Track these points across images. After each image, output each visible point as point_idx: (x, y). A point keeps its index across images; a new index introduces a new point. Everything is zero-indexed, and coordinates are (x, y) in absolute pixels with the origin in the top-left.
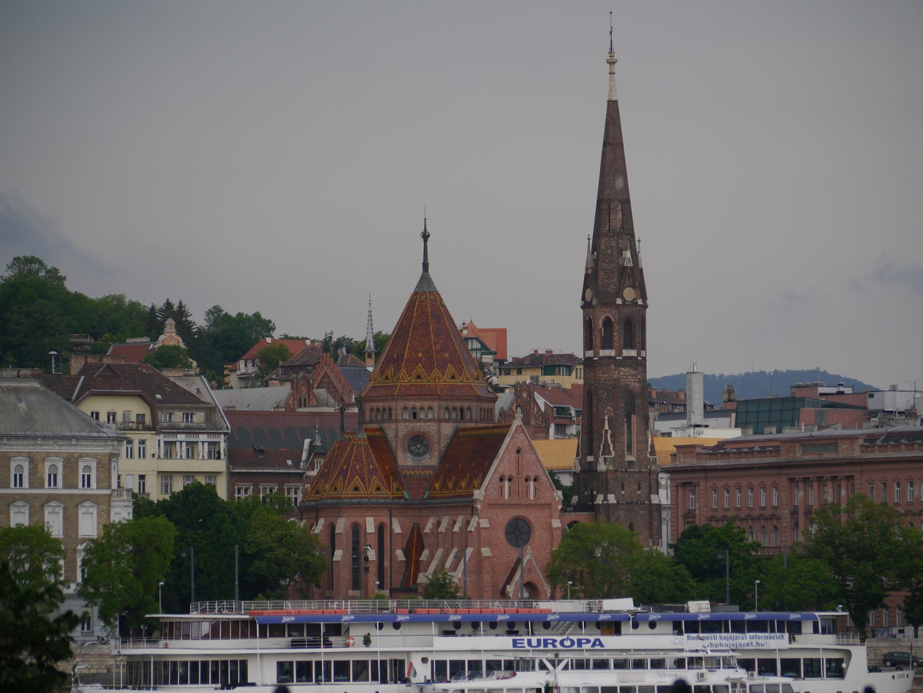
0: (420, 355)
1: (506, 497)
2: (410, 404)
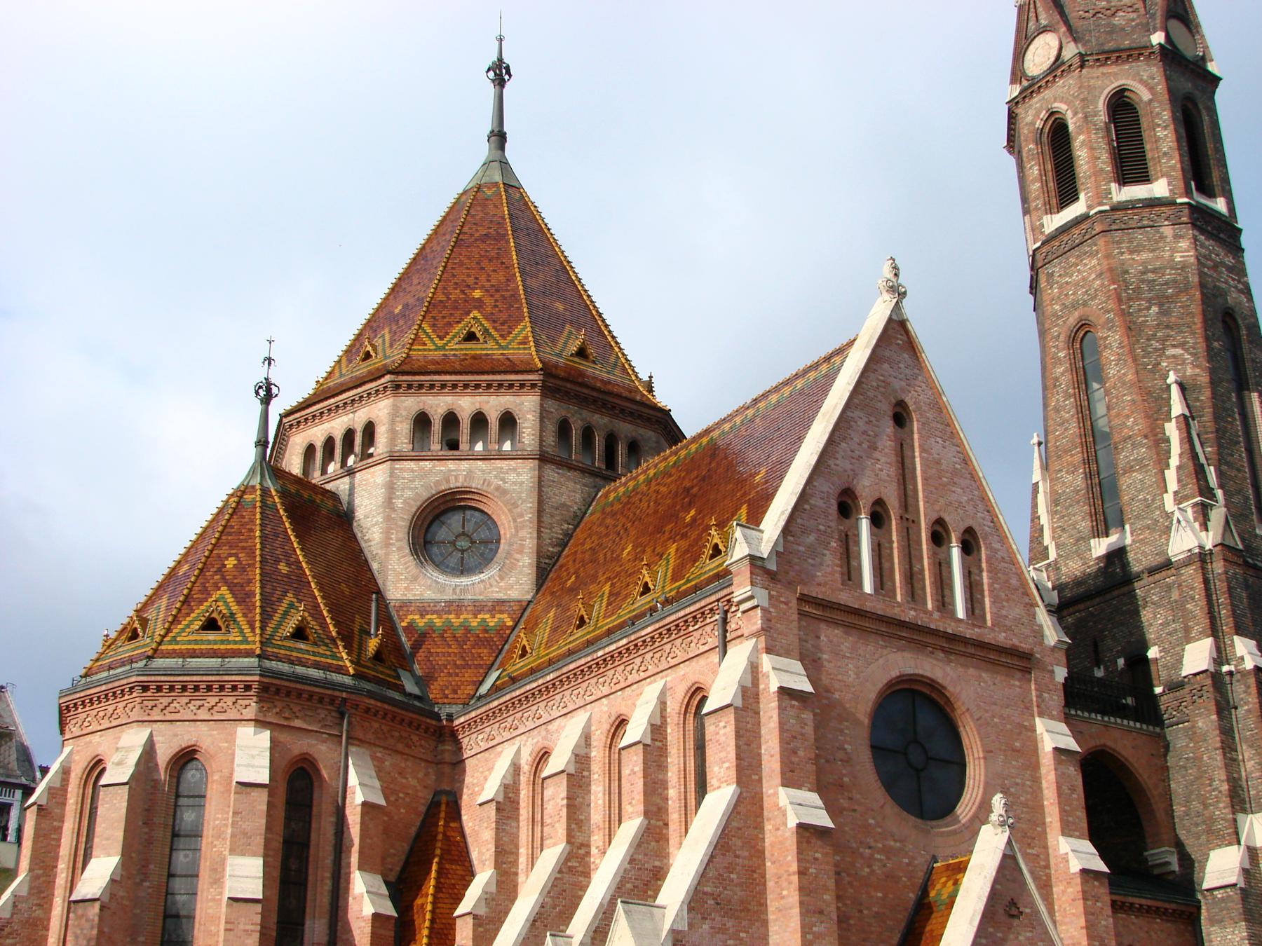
2: (437, 405)
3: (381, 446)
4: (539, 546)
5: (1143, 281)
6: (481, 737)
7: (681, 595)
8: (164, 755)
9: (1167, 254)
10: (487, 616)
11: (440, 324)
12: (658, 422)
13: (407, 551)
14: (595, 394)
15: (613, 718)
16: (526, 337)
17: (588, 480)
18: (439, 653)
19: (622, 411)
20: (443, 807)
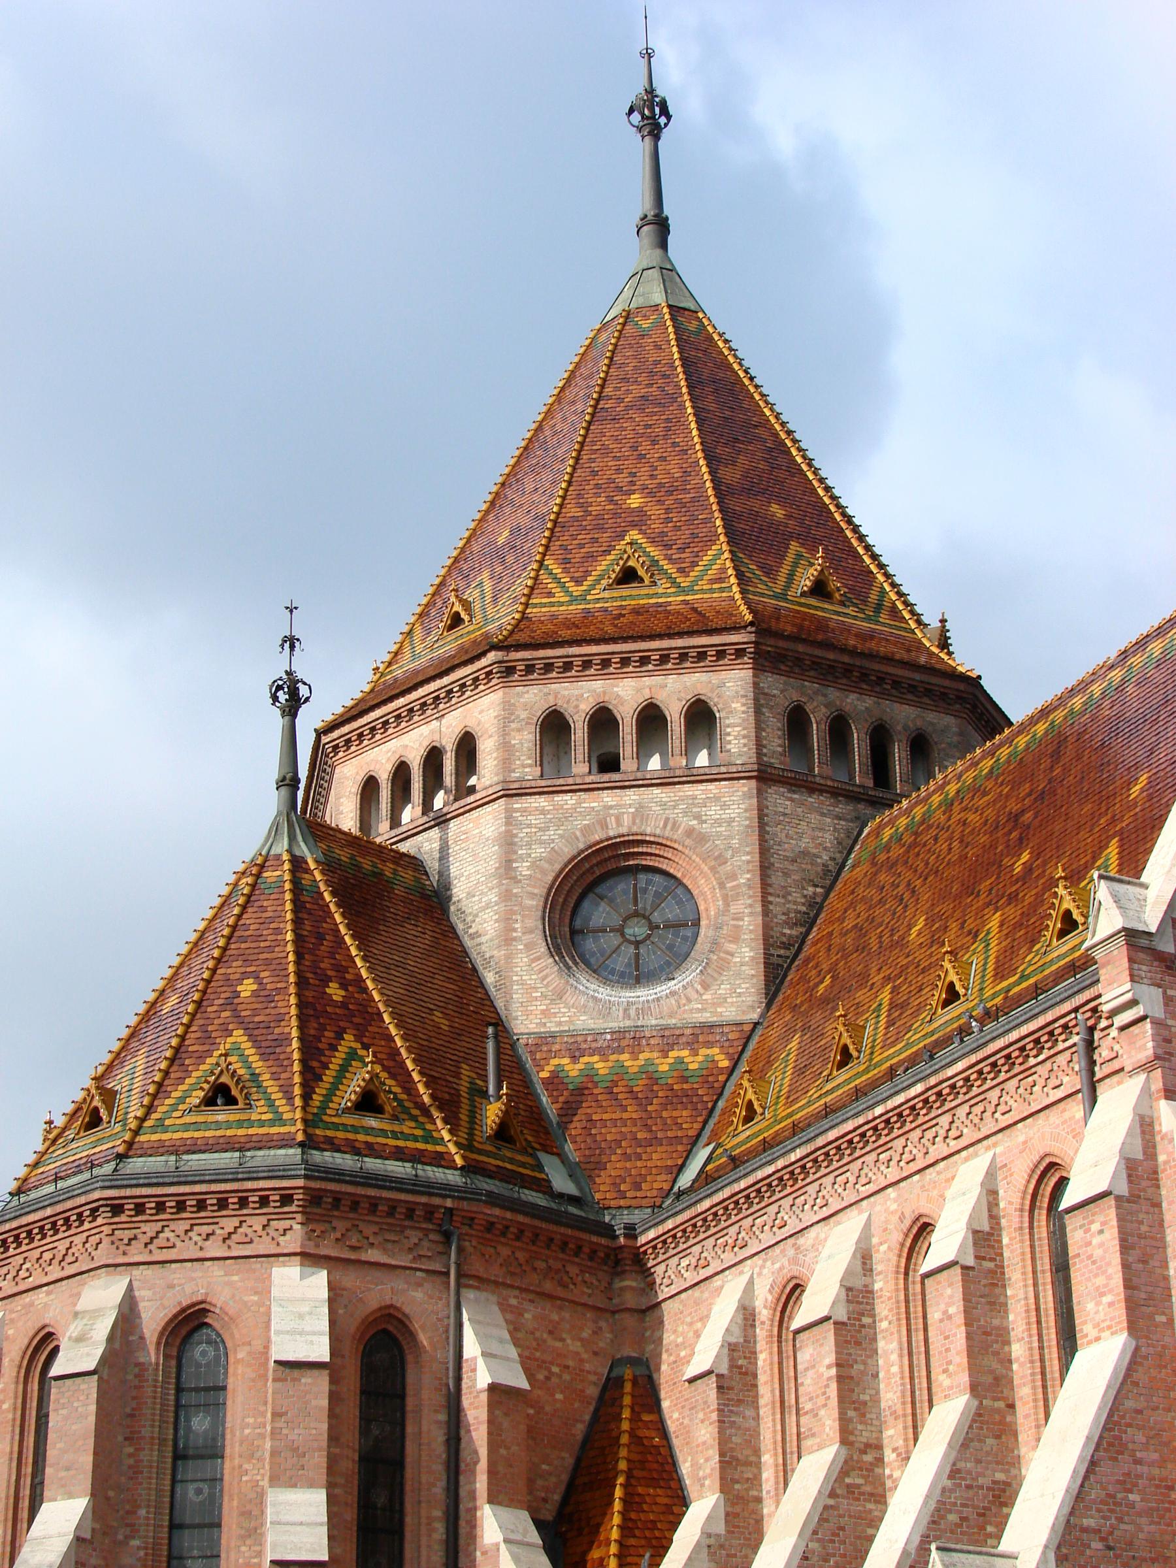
2: (578, 697)
4: (767, 927)
6: (684, 1263)
7: (1013, 1002)
8: (153, 1319)
10: (685, 1053)
11: (577, 557)
12: (960, 698)
13: (543, 949)
14: (846, 659)
15: (908, 1222)
16: (723, 570)
17: (843, 808)
18: (608, 1120)
19: (896, 684)
20: (628, 1387)
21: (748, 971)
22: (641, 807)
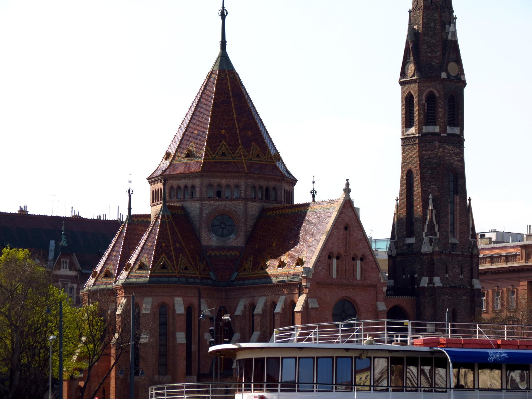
0: (223, 132)
1: (334, 276)
3: (197, 194)
5: (428, 161)
9: (436, 153)
21: (243, 237)
22: (225, 205)
